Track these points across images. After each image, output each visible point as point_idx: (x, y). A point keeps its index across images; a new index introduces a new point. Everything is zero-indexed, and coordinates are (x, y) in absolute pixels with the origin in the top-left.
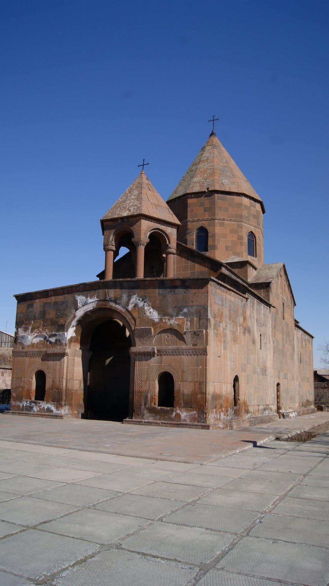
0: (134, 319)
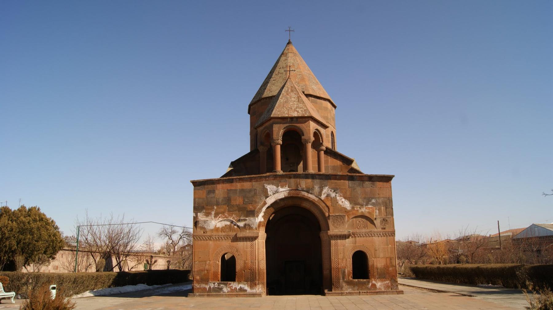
0: (327, 206)
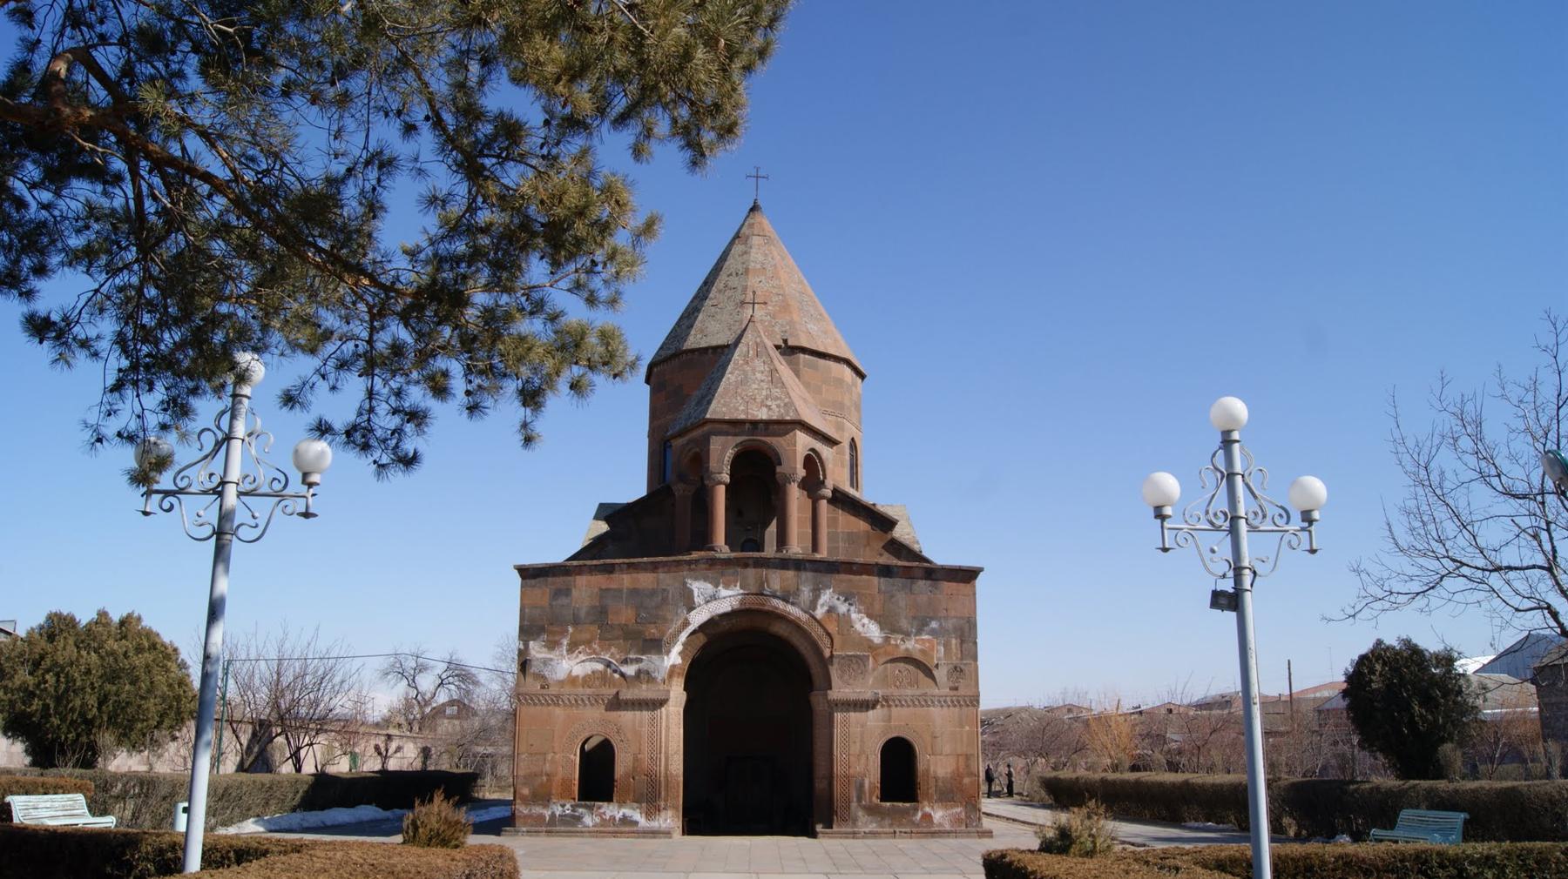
0: (829, 634)
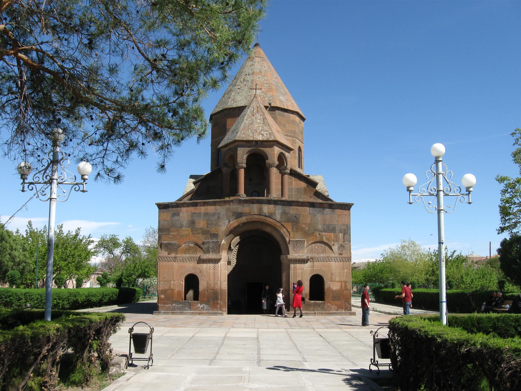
0: (288, 232)
